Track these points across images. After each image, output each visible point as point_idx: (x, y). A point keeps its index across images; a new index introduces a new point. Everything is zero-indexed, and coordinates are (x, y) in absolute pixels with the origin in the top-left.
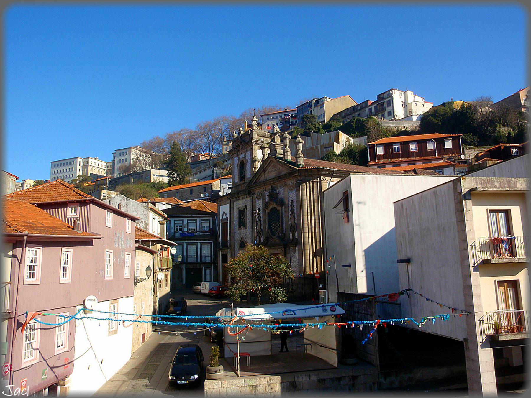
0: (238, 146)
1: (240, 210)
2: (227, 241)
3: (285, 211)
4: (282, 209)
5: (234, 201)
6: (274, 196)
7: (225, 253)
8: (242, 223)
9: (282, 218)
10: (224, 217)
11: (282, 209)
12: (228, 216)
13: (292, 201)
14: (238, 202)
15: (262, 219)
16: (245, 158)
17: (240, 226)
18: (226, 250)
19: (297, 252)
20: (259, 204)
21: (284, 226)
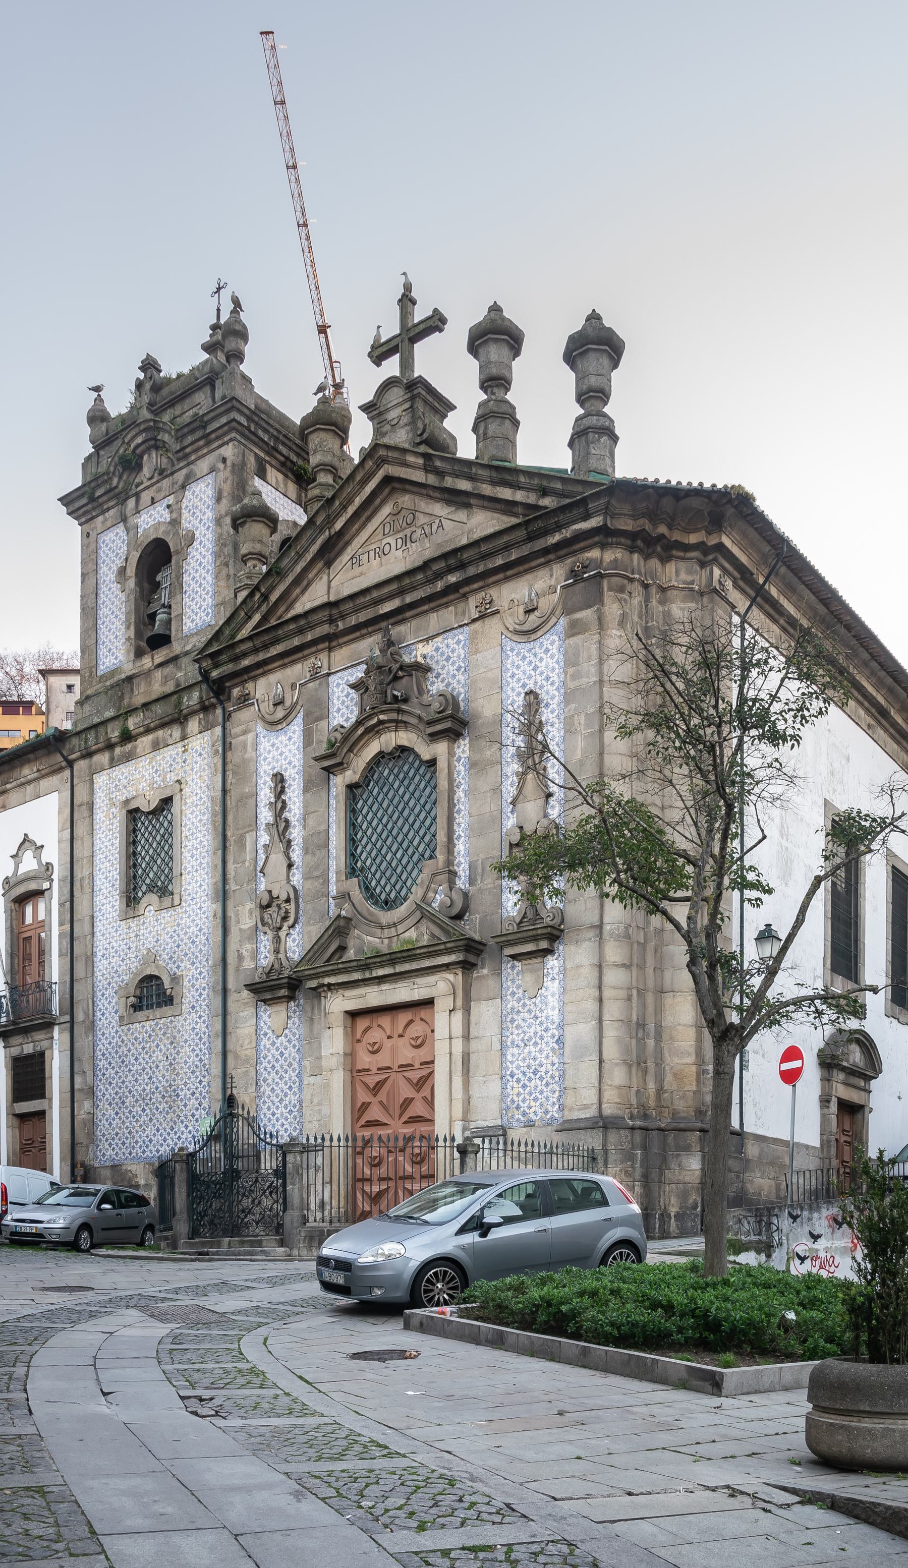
0: (131, 464)
1: (133, 814)
2: (42, 987)
3: (473, 765)
4: (451, 754)
5: (93, 772)
6: (392, 687)
7: (28, 1049)
8: (147, 878)
9: (451, 805)
10: (29, 864)
11: (451, 754)
12: (53, 854)
13: (533, 699)
14: (122, 772)
15: (296, 834)
16: (175, 523)
17: (131, 899)
18: (39, 1036)
19: (552, 987)
20: (280, 752)
21: (461, 847)
